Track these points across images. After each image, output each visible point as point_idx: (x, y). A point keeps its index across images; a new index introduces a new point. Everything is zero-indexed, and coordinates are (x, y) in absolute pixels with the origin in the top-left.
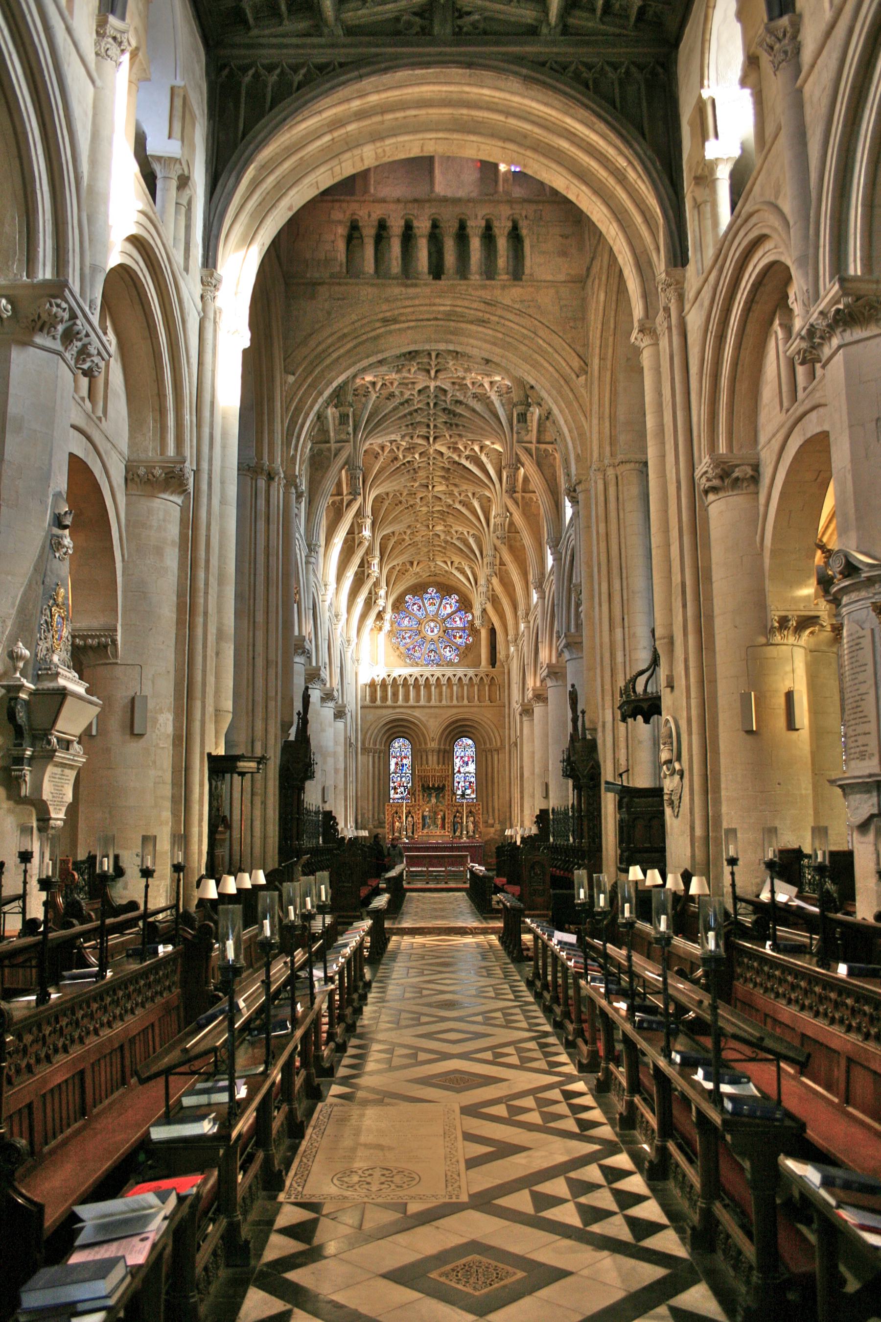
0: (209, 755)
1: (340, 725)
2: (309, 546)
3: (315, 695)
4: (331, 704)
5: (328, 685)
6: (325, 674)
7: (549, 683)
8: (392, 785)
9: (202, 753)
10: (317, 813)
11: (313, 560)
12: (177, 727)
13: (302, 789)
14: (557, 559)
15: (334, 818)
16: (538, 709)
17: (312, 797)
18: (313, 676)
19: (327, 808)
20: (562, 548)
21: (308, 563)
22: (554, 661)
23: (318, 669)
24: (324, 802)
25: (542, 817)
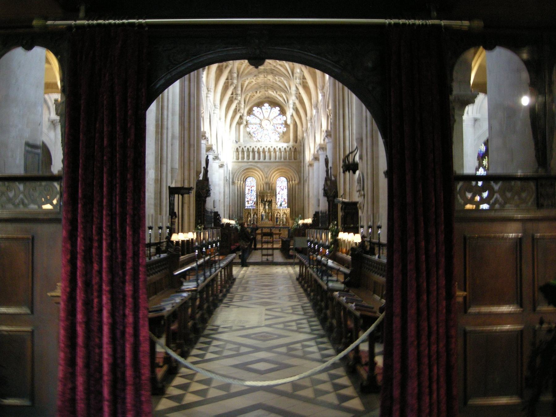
0: (169, 187)
1: (221, 170)
2: (208, 89)
3: (210, 158)
4: (217, 161)
5: (216, 152)
6: (214, 148)
7: (320, 152)
9: (166, 186)
10: (211, 212)
11: (209, 95)
12: (156, 176)
13: (205, 202)
14: (324, 96)
15: (219, 215)
16: (316, 164)
17: (209, 205)
18: (209, 149)
19: (216, 210)
20: (325, 90)
21: (207, 97)
22: (322, 142)
23: (212, 145)
24: (214, 207)
25: (316, 215)
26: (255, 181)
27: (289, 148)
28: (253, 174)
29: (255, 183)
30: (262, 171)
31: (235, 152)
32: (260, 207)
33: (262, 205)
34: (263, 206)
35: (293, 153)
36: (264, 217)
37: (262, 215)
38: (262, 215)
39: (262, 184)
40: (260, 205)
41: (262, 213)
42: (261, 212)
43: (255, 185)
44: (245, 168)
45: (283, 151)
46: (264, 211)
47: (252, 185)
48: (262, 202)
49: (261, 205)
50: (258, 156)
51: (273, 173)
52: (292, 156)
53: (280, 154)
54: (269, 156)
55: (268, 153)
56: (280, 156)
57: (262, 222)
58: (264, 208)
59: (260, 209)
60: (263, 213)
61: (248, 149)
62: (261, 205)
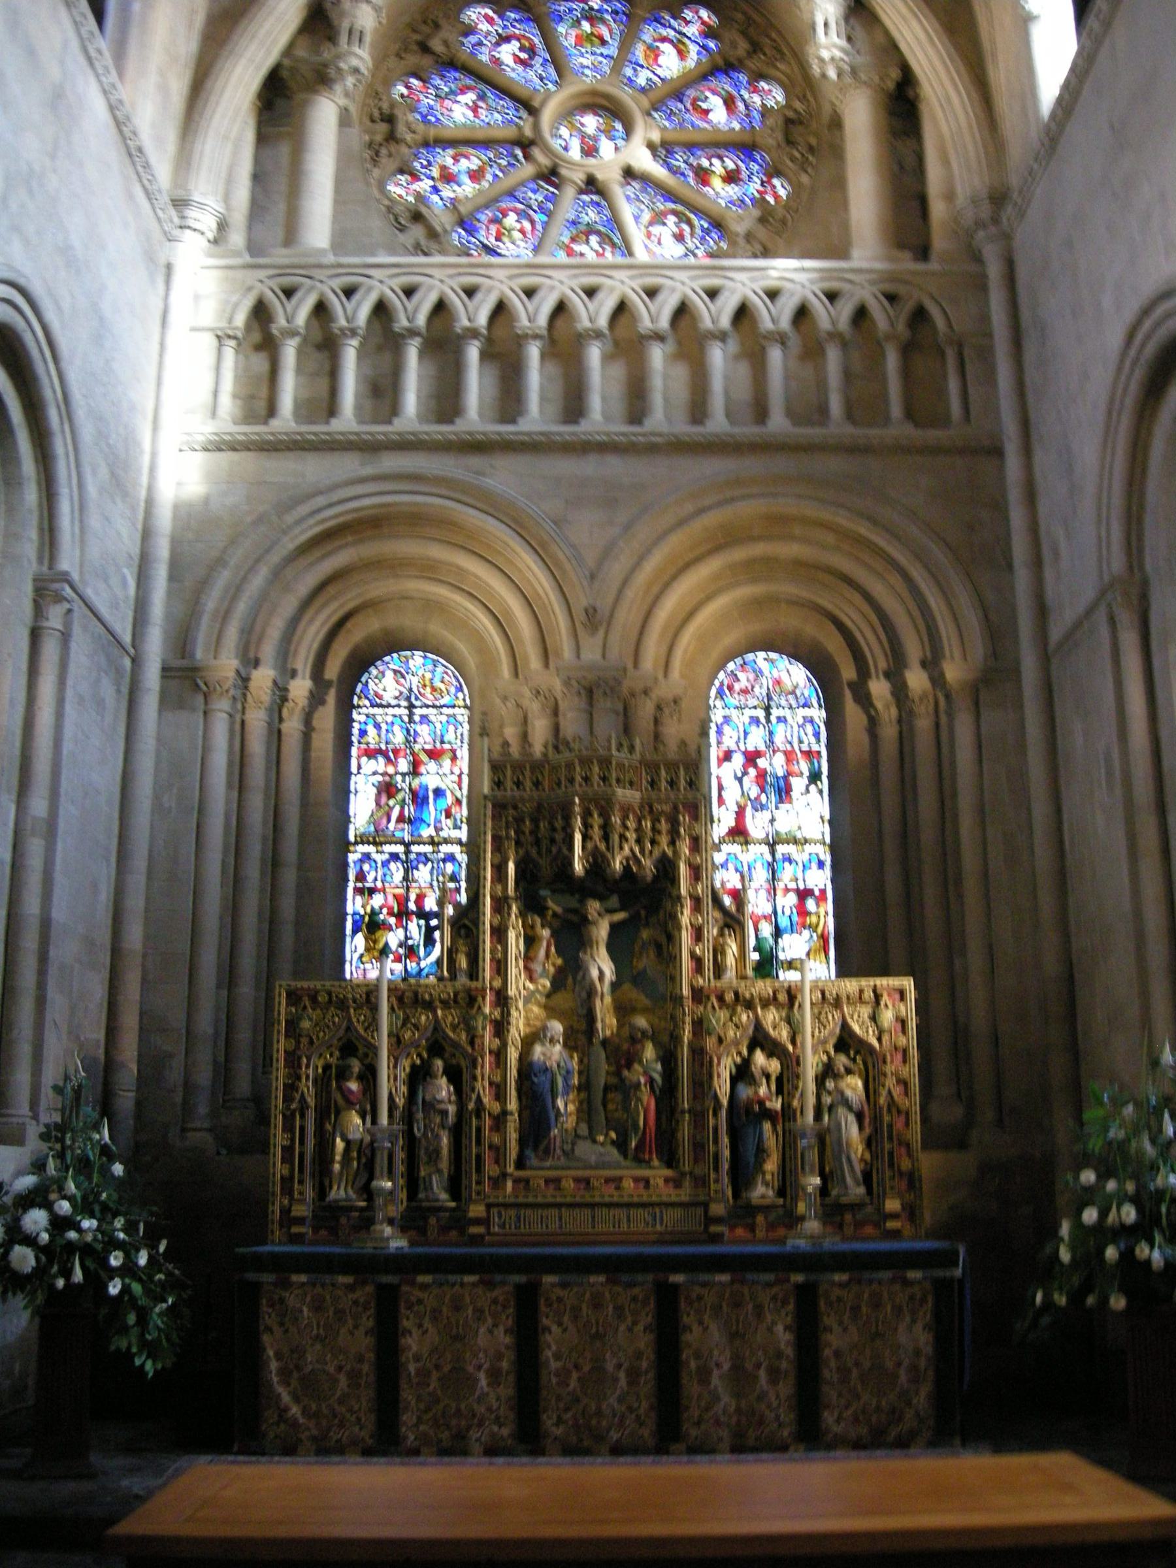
8: (354, 904)
26: (464, 697)
27: (845, 310)
28: (433, 607)
29: (462, 715)
30: (539, 550)
31: (229, 354)
32: (500, 967)
33: (531, 941)
34: (547, 960)
35: (892, 361)
36: (566, 1105)
37: (527, 1069)
38: (527, 1069)
39: (534, 707)
40: (500, 933)
41: (538, 1050)
42: (518, 1026)
43: (458, 736)
44: (331, 517)
45: (781, 339)
46: (557, 1027)
47: (425, 737)
48: (532, 905)
49: (515, 941)
50: (492, 391)
51: (666, 586)
52: (884, 397)
53: (743, 370)
54: (617, 389)
55: (607, 359)
56: (743, 392)
57: (537, 1175)
58: (558, 983)
59: (502, 999)
60: (550, 1053)
61: (381, 309)
62: (515, 941)
